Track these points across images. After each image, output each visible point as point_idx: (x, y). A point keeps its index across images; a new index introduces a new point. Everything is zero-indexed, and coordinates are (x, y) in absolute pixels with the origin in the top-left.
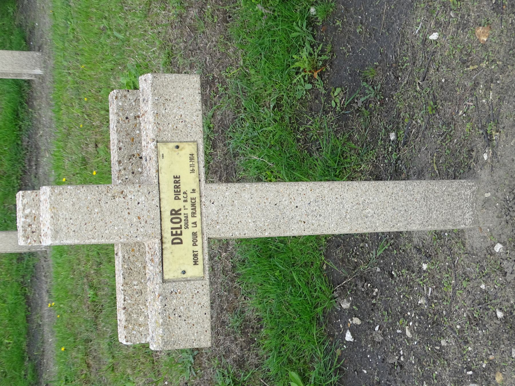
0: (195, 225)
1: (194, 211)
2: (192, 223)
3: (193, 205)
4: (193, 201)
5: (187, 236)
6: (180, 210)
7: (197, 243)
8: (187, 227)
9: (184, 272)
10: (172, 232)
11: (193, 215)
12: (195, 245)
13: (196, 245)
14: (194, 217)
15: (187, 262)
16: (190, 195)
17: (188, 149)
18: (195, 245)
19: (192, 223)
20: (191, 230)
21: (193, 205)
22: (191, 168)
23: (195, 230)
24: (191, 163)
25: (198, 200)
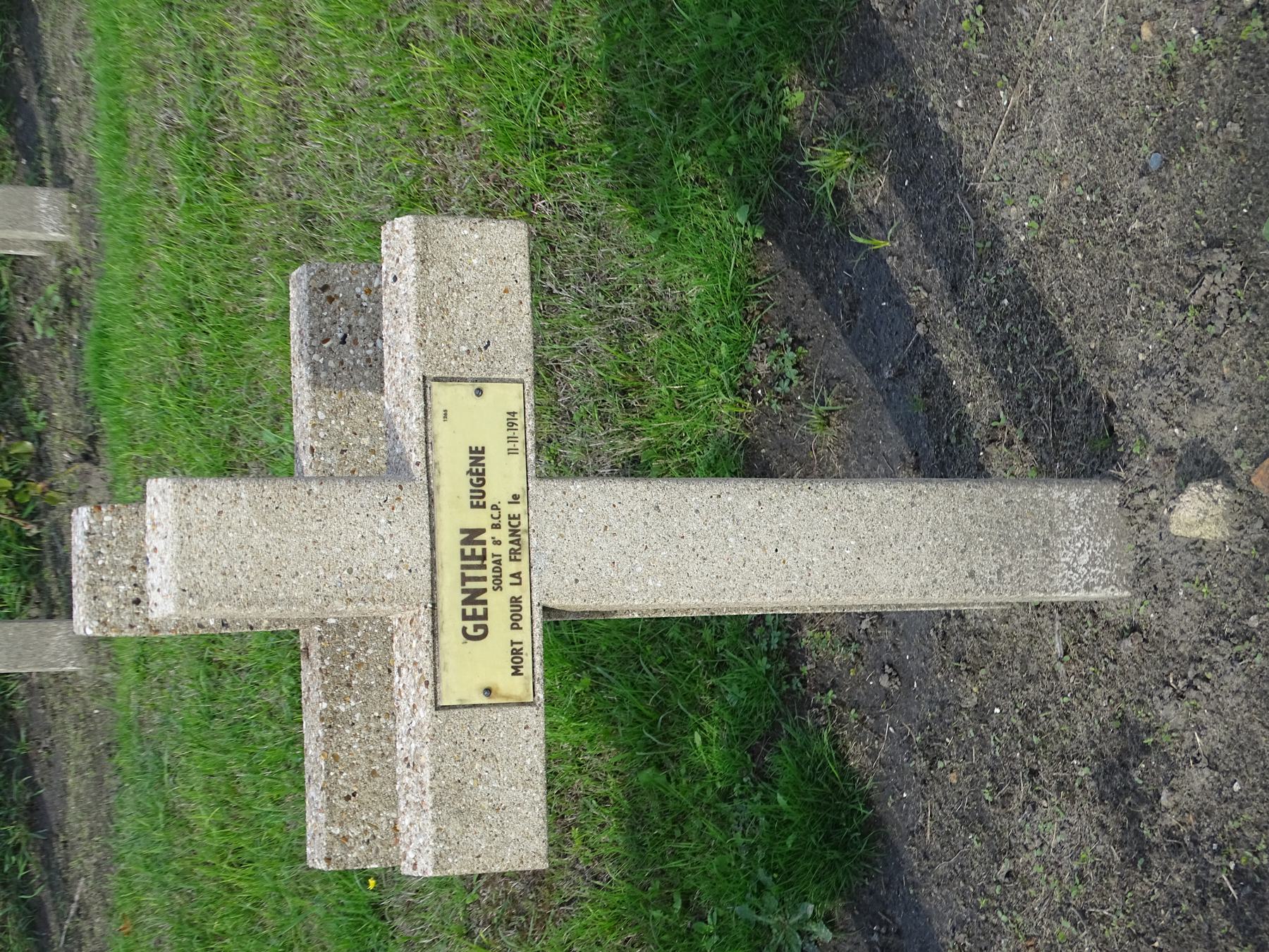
0: (517, 581)
1: (516, 547)
2: (513, 576)
4: (514, 522)
5: (498, 604)
6: (483, 531)
9: (488, 691)
11: (514, 555)
12: (515, 626)
14: (516, 560)
15: (495, 666)
16: (507, 510)
18: (515, 626)
19: (513, 576)
20: (510, 591)
21: (514, 532)
23: (516, 591)
24: (511, 433)
25: (524, 520)
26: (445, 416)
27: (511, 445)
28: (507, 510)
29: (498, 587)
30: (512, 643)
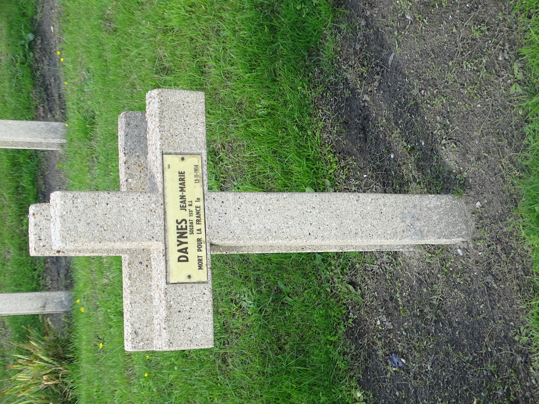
2: (198, 230)
3: (198, 213)
4: (198, 209)
8: (192, 233)
9: (189, 277)
11: (198, 222)
12: (199, 250)
13: (201, 251)
14: (199, 224)
16: (195, 204)
18: (199, 250)
19: (198, 230)
20: (196, 236)
21: (198, 213)
22: (196, 178)
23: (200, 236)
24: (195, 174)
26: (169, 167)
28: (195, 204)
30: (198, 257)
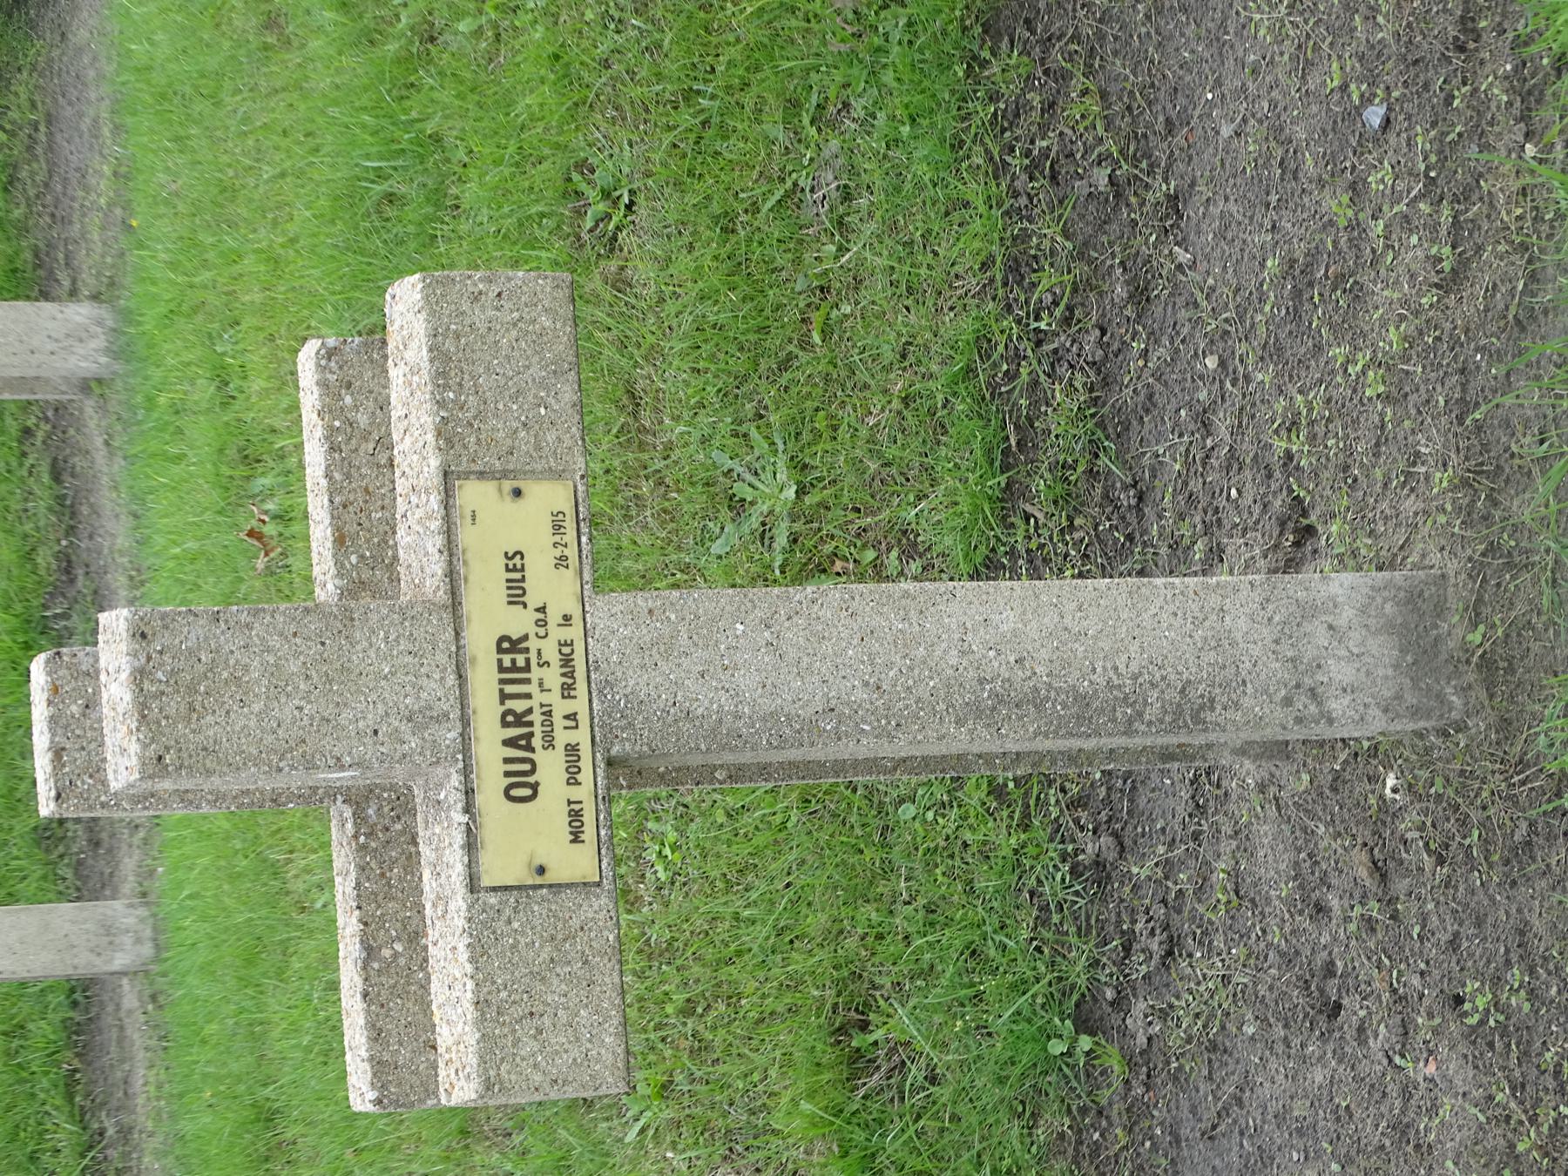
0: (573, 724)
1: (570, 681)
2: (567, 717)
3: (567, 661)
4: (566, 650)
6: (526, 638)
7: (579, 777)
10: (500, 661)
11: (567, 691)
12: (573, 781)
14: (570, 697)
17: (550, 497)
18: (573, 781)
19: (567, 717)
20: (562, 737)
21: (567, 661)
27: (558, 553)
29: (549, 744)
30: (569, 803)
